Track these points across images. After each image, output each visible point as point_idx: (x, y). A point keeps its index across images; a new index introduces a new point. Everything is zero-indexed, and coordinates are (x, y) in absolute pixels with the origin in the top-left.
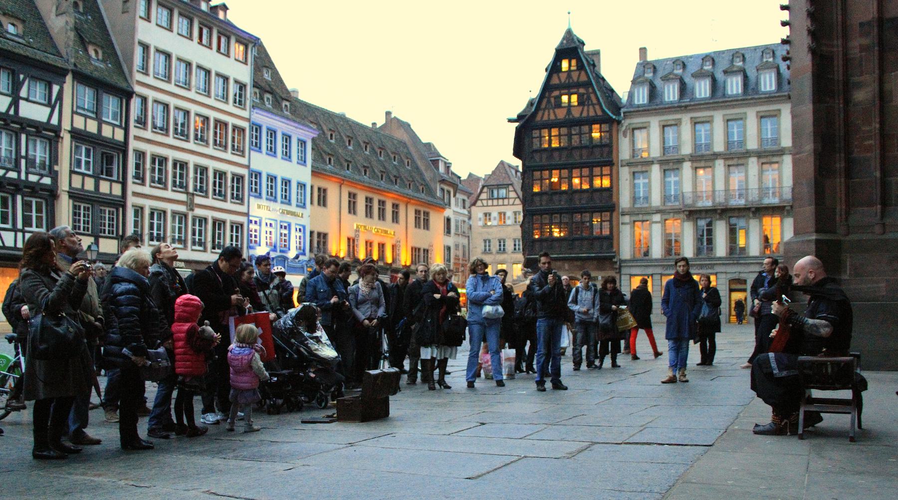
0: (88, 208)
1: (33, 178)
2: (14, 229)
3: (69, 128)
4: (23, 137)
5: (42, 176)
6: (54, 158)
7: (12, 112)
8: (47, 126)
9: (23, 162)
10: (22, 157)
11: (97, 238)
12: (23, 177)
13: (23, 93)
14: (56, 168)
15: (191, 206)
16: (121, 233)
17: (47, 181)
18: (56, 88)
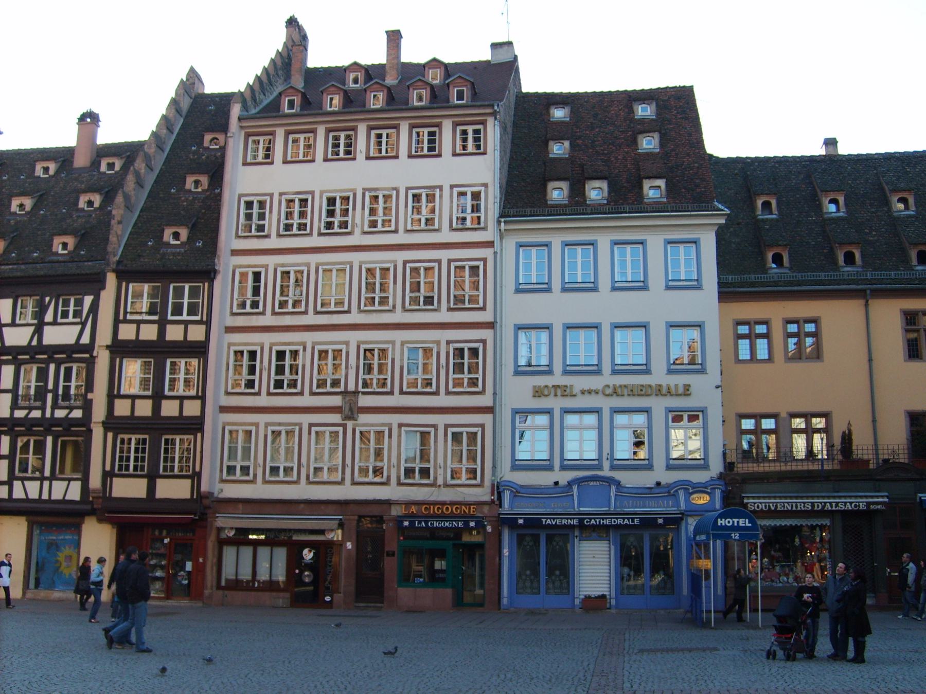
0: (144, 440)
1: (60, 414)
2: (42, 479)
3: (109, 342)
4: (52, 367)
5: (71, 409)
6: (90, 385)
7: (34, 343)
8: (77, 347)
9: (50, 396)
10: (50, 391)
11: (152, 478)
12: (48, 415)
13: (49, 317)
14: (90, 396)
15: (351, 411)
16: (197, 469)
17: (77, 414)
18: (88, 300)
